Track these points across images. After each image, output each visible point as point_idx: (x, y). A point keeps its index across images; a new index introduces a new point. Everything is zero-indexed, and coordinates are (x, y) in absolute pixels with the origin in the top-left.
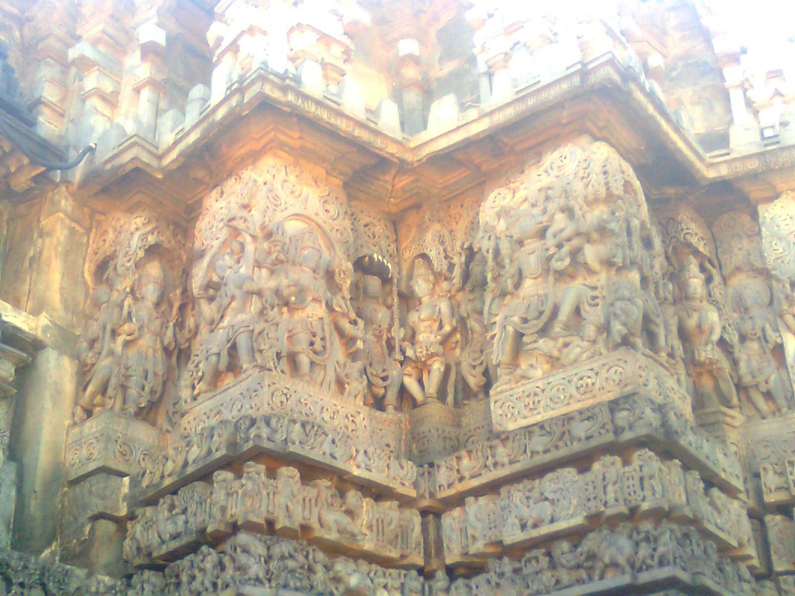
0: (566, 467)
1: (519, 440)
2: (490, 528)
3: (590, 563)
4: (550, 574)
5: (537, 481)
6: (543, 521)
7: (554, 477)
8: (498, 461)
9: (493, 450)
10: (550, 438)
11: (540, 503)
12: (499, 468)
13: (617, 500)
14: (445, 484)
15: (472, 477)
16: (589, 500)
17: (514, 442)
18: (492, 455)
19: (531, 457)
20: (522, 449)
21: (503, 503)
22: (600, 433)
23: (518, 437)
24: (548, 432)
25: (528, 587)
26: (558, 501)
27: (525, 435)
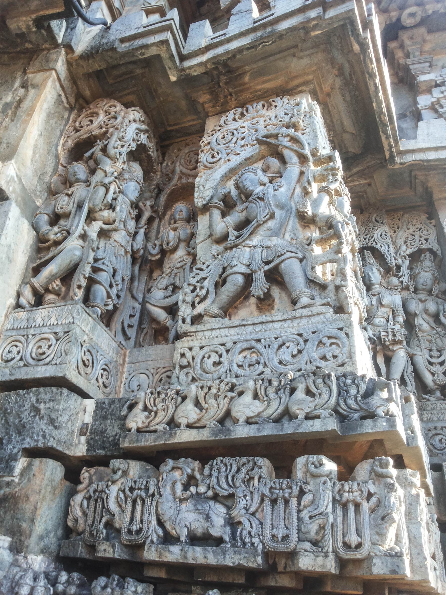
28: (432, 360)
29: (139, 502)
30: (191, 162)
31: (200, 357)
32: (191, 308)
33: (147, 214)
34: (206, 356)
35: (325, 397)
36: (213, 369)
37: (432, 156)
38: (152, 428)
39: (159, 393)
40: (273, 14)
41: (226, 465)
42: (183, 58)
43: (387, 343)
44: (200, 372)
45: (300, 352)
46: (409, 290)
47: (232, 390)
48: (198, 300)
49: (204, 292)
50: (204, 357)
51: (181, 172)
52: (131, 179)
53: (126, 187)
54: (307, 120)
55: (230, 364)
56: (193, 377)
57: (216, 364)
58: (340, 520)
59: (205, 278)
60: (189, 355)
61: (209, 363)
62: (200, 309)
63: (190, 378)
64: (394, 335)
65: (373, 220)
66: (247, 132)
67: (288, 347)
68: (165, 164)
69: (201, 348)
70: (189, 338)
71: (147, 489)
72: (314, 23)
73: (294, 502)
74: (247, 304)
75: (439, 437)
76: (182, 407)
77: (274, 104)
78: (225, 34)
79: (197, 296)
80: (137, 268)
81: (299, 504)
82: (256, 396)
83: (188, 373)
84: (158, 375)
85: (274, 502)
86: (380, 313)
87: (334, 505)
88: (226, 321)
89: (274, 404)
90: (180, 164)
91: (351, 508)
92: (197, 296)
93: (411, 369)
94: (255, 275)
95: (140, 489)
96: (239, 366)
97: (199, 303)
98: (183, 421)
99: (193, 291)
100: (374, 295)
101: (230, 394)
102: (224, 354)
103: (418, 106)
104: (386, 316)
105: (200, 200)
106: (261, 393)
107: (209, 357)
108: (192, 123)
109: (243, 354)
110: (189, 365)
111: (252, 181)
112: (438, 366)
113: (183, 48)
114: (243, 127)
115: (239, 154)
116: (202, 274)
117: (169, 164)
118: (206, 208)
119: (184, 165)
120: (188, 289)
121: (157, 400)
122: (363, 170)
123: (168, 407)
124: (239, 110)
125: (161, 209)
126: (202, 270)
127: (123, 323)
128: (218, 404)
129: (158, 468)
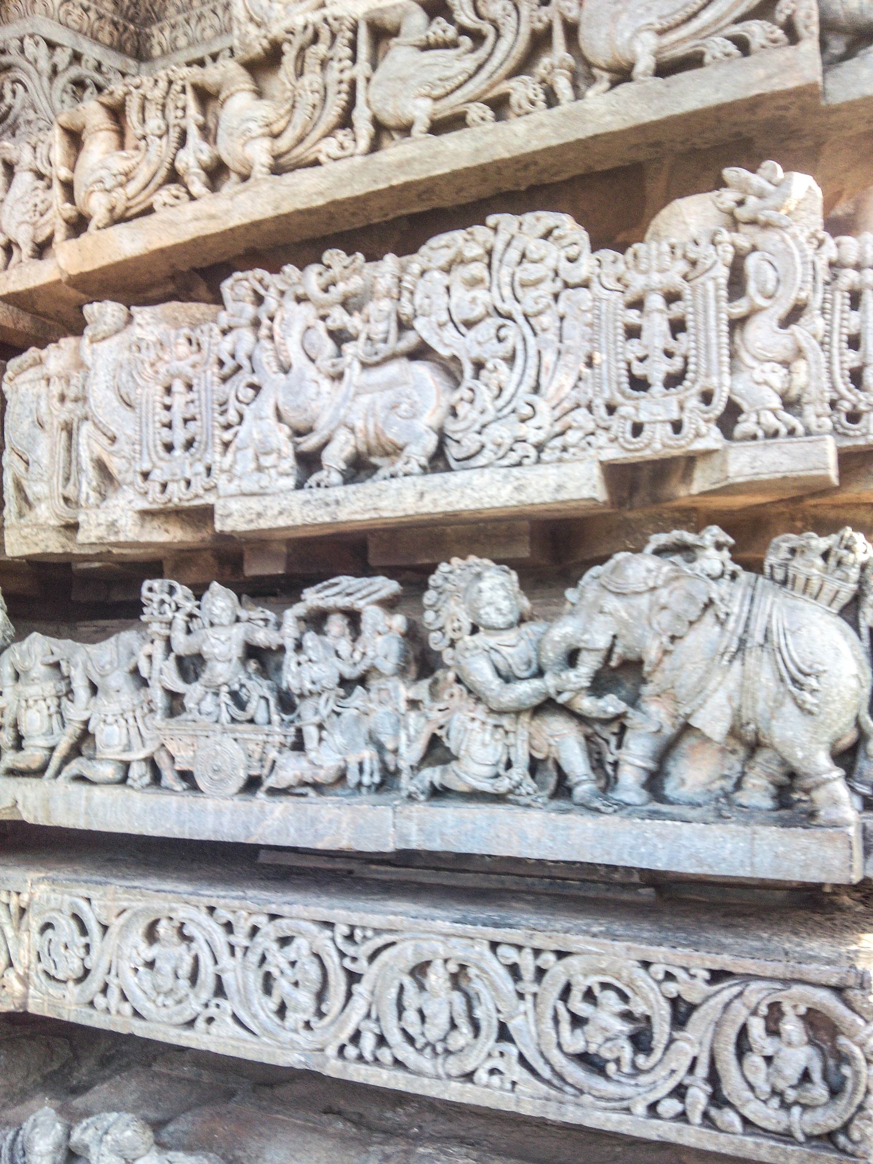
0: (532, 208)
1: (324, 64)
2: (169, 448)
3: (611, 704)
4: (404, 691)
5: (390, 261)
6: (395, 451)
8: (227, 159)
9: (212, 106)
10: (469, 63)
11: (393, 369)
12: (231, 185)
13: (791, 404)
14: (24, 238)
15: (118, 219)
16: (639, 384)
17: (300, 73)
18: (204, 129)
19: (375, 146)
20: (332, 112)
21: (226, 345)
22: (743, 45)
23: (321, 49)
24: (463, 31)
25: (299, 746)
26: (479, 366)
27: (353, 45)
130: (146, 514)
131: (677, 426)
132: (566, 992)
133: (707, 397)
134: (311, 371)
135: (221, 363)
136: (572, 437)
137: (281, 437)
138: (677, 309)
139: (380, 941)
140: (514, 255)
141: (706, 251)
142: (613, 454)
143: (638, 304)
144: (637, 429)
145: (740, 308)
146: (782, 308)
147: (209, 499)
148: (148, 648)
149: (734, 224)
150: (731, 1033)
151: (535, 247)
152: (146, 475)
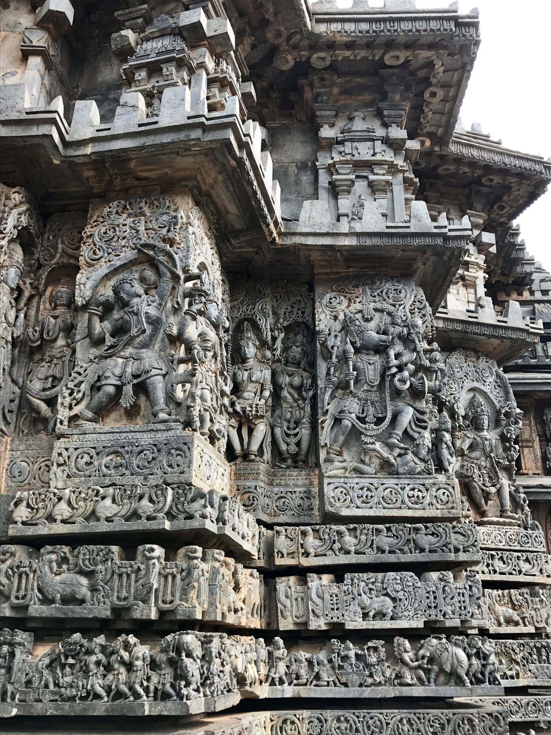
7: (398, 578)
16: (430, 607)
22: (443, 550)
24: (394, 535)
27: (372, 532)
28: (289, 432)
29: (24, 576)
30: (73, 240)
31: (75, 457)
32: (68, 410)
33: (27, 294)
34: (80, 456)
35: (161, 505)
36: (85, 467)
37: (310, 241)
38: (34, 522)
39: (40, 494)
40: (156, 123)
41: (89, 551)
42: (66, 144)
43: (251, 417)
44: (75, 470)
45: (154, 459)
46: (281, 362)
47: (97, 495)
48: (74, 402)
49: (80, 395)
50: (77, 458)
51: (63, 250)
52: (12, 266)
53: (7, 274)
54: (183, 233)
55: (100, 465)
56: (68, 474)
57: (87, 464)
58: (162, 586)
59: (81, 382)
60: (65, 454)
61: (82, 462)
62: (76, 410)
63: (66, 475)
64: (257, 411)
65: (257, 290)
66: (128, 231)
67: (145, 455)
68: (46, 236)
69: (76, 449)
70: (66, 440)
71: (31, 567)
72: (193, 142)
73: (133, 576)
74: (118, 408)
75: (283, 500)
76: (58, 506)
77: (156, 203)
78: (109, 129)
79: (74, 399)
80: (16, 351)
81: (136, 577)
82: (114, 501)
83: (64, 470)
84: (38, 463)
85: (120, 575)
86: (249, 388)
87: (159, 578)
88: (97, 426)
89: (126, 507)
90: (63, 242)
91: (170, 578)
92: (74, 399)
93: (269, 440)
94: (124, 388)
95: (24, 567)
96: (106, 467)
97: (76, 405)
98: (59, 518)
99: (70, 395)
100: (246, 370)
101: (95, 498)
102: (95, 456)
103: (317, 163)
104: (254, 390)
105: (80, 299)
106: (118, 499)
107: (82, 457)
108: (76, 189)
109: (110, 457)
110: (65, 463)
111: (128, 294)
112: (292, 437)
113: (67, 133)
114: (125, 225)
115: (119, 255)
116: (80, 378)
117: (51, 238)
118: (85, 307)
119: (67, 243)
120: (66, 393)
121: (38, 500)
122: (250, 240)
123: (47, 506)
124: (123, 202)
125: (41, 287)
126: (80, 374)
127: (3, 408)
128: (86, 506)
129: (39, 550)
130: (325, 623)
131: (436, 616)
132: (429, 721)
133: (441, 611)
134: (365, 597)
135: (345, 592)
136: (419, 616)
137: (359, 610)
138: (435, 595)
139: (393, 715)
140: (406, 580)
141: (439, 586)
142: (426, 619)
143: (428, 592)
144: (430, 615)
145: (444, 596)
146: (450, 597)
147: (343, 622)
148: (333, 655)
149: (441, 579)
150: (457, 724)
151: (409, 579)
152: (327, 615)
